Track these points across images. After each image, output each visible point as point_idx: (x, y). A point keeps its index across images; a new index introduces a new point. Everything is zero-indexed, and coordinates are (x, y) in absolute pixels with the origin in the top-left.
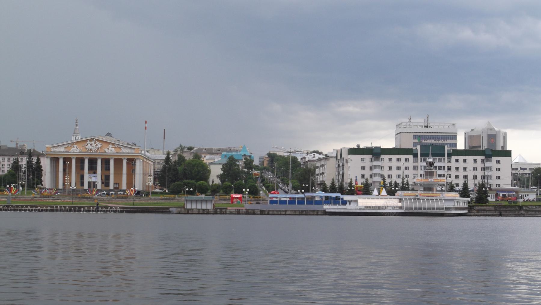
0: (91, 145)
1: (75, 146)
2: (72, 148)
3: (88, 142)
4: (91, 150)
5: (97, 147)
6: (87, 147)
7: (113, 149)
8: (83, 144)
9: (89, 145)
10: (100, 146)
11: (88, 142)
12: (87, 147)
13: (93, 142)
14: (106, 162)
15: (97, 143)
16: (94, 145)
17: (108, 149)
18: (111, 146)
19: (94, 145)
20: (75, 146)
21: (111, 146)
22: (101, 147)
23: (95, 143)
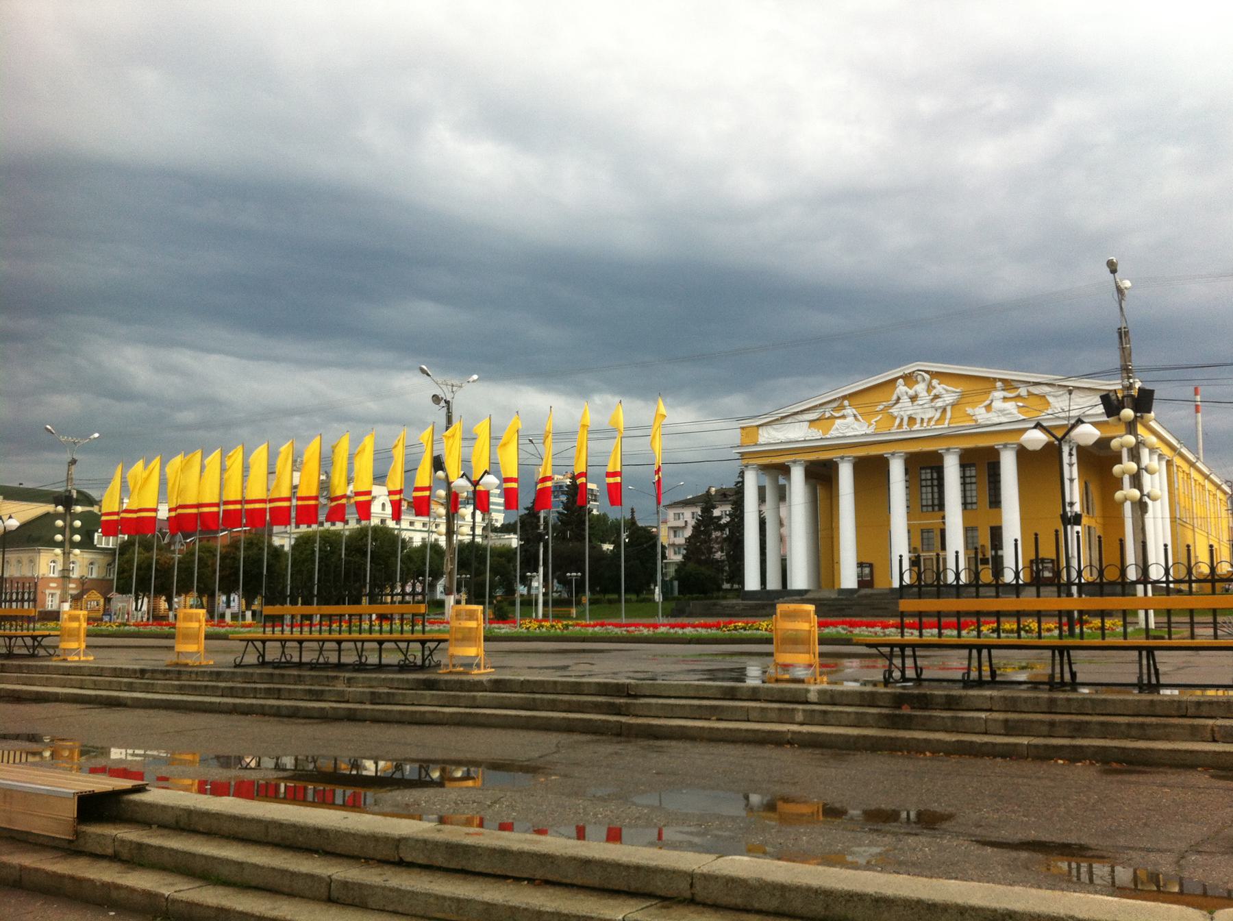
0: (913, 399)
1: (849, 411)
2: (838, 421)
3: (901, 388)
5: (939, 403)
6: (894, 411)
9: (905, 399)
11: (901, 388)
13: (920, 388)
14: (981, 464)
15: (939, 388)
17: (988, 408)
20: (849, 411)
22: (953, 405)
23: (930, 387)
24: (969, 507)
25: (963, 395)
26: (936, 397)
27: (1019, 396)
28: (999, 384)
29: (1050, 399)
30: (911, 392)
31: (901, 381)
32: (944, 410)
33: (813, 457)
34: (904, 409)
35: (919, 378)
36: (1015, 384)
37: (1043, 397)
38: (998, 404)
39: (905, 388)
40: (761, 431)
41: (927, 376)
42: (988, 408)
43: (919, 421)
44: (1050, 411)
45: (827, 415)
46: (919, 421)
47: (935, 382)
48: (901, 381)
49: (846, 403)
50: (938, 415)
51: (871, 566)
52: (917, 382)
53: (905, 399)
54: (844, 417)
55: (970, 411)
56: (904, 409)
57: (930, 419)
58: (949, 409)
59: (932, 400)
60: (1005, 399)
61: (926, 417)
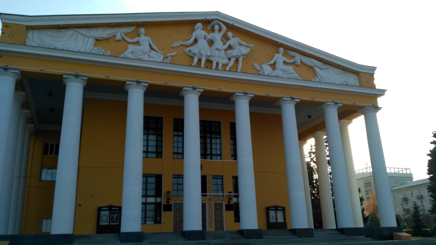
0: (211, 43)
1: (145, 40)
2: (131, 48)
3: (199, 32)
4: (209, 62)
6: (194, 49)
7: (290, 68)
9: (203, 44)
10: (245, 51)
11: (199, 32)
12: (194, 49)
13: (217, 36)
15: (234, 40)
17: (273, 66)
18: (279, 58)
19: (219, 44)
20: (145, 40)
21: (279, 58)
23: (225, 38)
24: (214, 157)
26: (230, 47)
28: (281, 50)
29: (317, 69)
30: (210, 36)
31: (200, 25)
32: (237, 60)
34: (202, 48)
35: (217, 27)
37: (312, 67)
38: (280, 65)
39: (204, 33)
40: (30, 34)
41: (224, 28)
42: (273, 66)
44: (317, 80)
45: (119, 37)
47: (230, 34)
48: (200, 25)
49: (142, 30)
50: (232, 63)
52: (213, 30)
53: (203, 44)
54: (138, 43)
55: (257, 66)
57: (225, 65)
58: (241, 59)
59: (226, 50)
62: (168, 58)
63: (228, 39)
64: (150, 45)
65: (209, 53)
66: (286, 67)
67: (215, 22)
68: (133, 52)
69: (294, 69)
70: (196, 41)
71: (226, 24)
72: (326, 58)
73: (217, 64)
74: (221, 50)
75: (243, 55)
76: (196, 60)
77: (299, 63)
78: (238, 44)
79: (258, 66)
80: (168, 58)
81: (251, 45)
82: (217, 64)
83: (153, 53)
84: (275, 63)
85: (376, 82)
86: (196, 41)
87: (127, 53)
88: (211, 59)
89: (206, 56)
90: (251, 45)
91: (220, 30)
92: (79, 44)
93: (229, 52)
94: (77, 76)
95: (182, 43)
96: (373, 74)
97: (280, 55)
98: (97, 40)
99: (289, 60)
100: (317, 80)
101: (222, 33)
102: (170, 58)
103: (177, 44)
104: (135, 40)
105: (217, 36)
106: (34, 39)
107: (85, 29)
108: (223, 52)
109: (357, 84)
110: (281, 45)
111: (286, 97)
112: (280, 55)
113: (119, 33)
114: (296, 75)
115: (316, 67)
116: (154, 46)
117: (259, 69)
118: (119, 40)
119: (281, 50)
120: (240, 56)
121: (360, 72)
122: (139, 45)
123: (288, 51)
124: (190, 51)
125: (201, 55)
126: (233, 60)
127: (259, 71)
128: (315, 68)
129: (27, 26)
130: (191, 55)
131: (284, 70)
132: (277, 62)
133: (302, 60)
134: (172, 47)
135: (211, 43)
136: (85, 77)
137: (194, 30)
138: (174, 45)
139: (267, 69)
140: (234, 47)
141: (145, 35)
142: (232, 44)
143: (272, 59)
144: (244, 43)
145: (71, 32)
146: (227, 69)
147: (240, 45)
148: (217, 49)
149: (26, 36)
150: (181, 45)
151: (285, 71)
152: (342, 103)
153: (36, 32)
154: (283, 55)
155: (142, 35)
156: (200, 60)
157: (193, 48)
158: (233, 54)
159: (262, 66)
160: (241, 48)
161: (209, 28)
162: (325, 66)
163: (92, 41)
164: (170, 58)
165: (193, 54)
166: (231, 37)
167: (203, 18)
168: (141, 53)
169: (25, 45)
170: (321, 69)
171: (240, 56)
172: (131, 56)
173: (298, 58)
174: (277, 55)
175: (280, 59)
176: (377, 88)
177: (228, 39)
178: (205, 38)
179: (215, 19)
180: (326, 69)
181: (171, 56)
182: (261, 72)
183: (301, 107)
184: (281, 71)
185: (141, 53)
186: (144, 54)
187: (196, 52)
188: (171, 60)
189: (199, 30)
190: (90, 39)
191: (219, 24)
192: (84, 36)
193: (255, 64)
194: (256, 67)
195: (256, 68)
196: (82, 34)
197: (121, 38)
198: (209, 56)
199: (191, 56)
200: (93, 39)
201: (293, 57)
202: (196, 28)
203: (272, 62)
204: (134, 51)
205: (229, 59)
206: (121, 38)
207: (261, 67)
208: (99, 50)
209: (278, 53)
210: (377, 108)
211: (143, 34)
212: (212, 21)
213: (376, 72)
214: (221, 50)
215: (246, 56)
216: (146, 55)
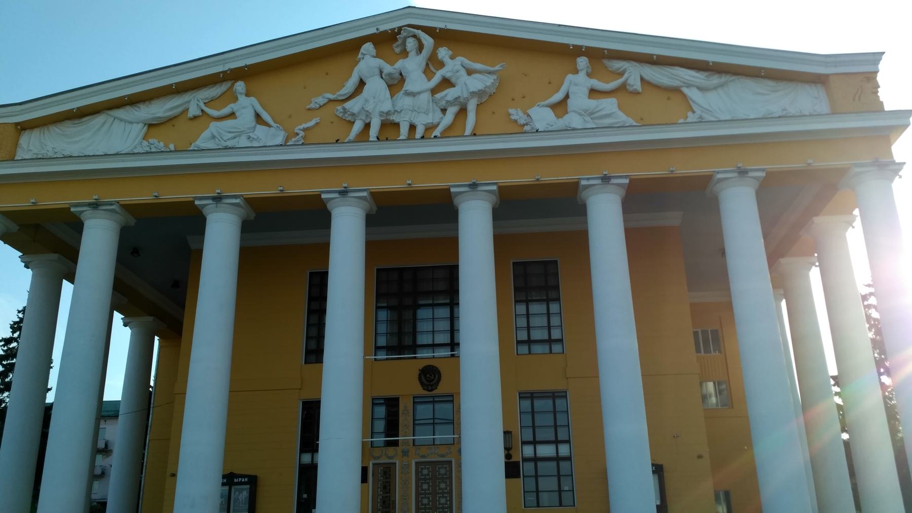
0: (396, 84)
3: (369, 62)
7: (609, 104)
8: (317, 90)
9: (376, 87)
10: (477, 83)
11: (369, 62)
13: (413, 65)
15: (453, 64)
16: (417, 81)
17: (561, 107)
18: (578, 83)
19: (417, 81)
20: (246, 106)
23: (433, 63)
25: (501, 84)
26: (447, 83)
27: (623, 88)
28: (582, 62)
31: (368, 47)
32: (463, 111)
33: (142, 195)
34: (376, 100)
35: (411, 44)
36: (617, 65)
37: (677, 90)
38: (580, 100)
39: (379, 62)
41: (428, 41)
42: (561, 107)
43: (404, 130)
45: (193, 111)
46: (404, 130)
47: (443, 53)
48: (368, 47)
49: (240, 86)
51: (253, 481)
52: (405, 54)
54: (232, 115)
55: (517, 114)
56: (376, 100)
57: (430, 128)
58: (472, 107)
59: (434, 91)
60: (594, 93)
61: (421, 122)
62: (297, 134)
63: (441, 64)
64: (258, 116)
65: (387, 106)
66: (593, 103)
67: (403, 34)
68: (214, 137)
69: (620, 107)
70: (362, 83)
71: (429, 31)
72: (711, 58)
73: (413, 127)
74: (419, 93)
75: (473, 94)
76: (358, 126)
77: (638, 86)
78: (463, 72)
79: (521, 114)
80: (297, 134)
81: (497, 68)
82: (413, 127)
83: (261, 130)
84: (567, 96)
85: (882, 94)
86: (362, 83)
87: (202, 142)
88: (395, 118)
89: (381, 116)
90: (497, 68)
91: (420, 48)
92: (115, 140)
93: (438, 96)
94: (95, 205)
95: (331, 97)
96: (877, 72)
97: (581, 77)
98: (151, 126)
99: (607, 83)
100: (691, 117)
101: (426, 52)
102: (302, 134)
103: (321, 100)
104: (226, 111)
105: (413, 65)
106: (31, 144)
107: (128, 108)
108: (426, 96)
109: (823, 107)
110: (578, 51)
111: (588, 179)
112: (581, 77)
113: (194, 102)
114: (622, 118)
115: (689, 86)
116: (266, 116)
117: (522, 122)
118: (195, 118)
119: (582, 62)
120: (467, 100)
121: (827, 76)
122: (236, 118)
123: (606, 62)
124: (345, 111)
125: (368, 114)
126: (452, 111)
127: (524, 125)
128: (685, 90)
129: (17, 124)
130: (349, 118)
131: (585, 111)
132: (571, 96)
133: (646, 77)
134: (309, 109)
135: (396, 84)
136: (111, 204)
137: (357, 62)
138: (312, 105)
139: (542, 117)
140: (453, 80)
141: (248, 95)
142: (448, 75)
143: (557, 91)
144: (478, 66)
145: (100, 119)
146: (437, 132)
147: (470, 72)
148: (408, 94)
149: (16, 144)
150: (330, 101)
151: (592, 113)
152: (763, 170)
153: (36, 133)
154: (589, 75)
155: (239, 96)
156: (367, 126)
157: (354, 105)
158: (449, 98)
159: (529, 111)
160: (470, 78)
161: (397, 50)
162: (715, 80)
163: (138, 130)
164: (302, 134)
165: (353, 114)
166: (447, 60)
167: (372, 31)
168: (233, 135)
169: (13, 160)
170: (700, 89)
171: (467, 100)
172: (211, 145)
173: (634, 74)
174: (570, 77)
175: (576, 85)
176: (887, 108)
177: (441, 64)
178: (381, 72)
179: (400, 28)
180: (721, 86)
181: (304, 130)
182: (527, 128)
183: (639, 198)
184: (580, 114)
185: (233, 135)
186: (239, 136)
187: (356, 110)
188: (304, 138)
189: (367, 57)
190: (135, 125)
191: (415, 36)
192: (125, 121)
193: (511, 111)
194: (513, 118)
195: (515, 121)
196: (121, 120)
197: (199, 113)
198: (388, 113)
199: (349, 121)
200: (141, 125)
201: (621, 74)
202: (360, 56)
203: (558, 97)
204: (216, 134)
205: (444, 111)
206: (199, 113)
207: (528, 115)
208: (157, 144)
209: (576, 71)
210: (895, 168)
211: (241, 94)
212: (399, 33)
213: (881, 66)
214: (419, 93)
215: (485, 99)
216: (244, 137)
